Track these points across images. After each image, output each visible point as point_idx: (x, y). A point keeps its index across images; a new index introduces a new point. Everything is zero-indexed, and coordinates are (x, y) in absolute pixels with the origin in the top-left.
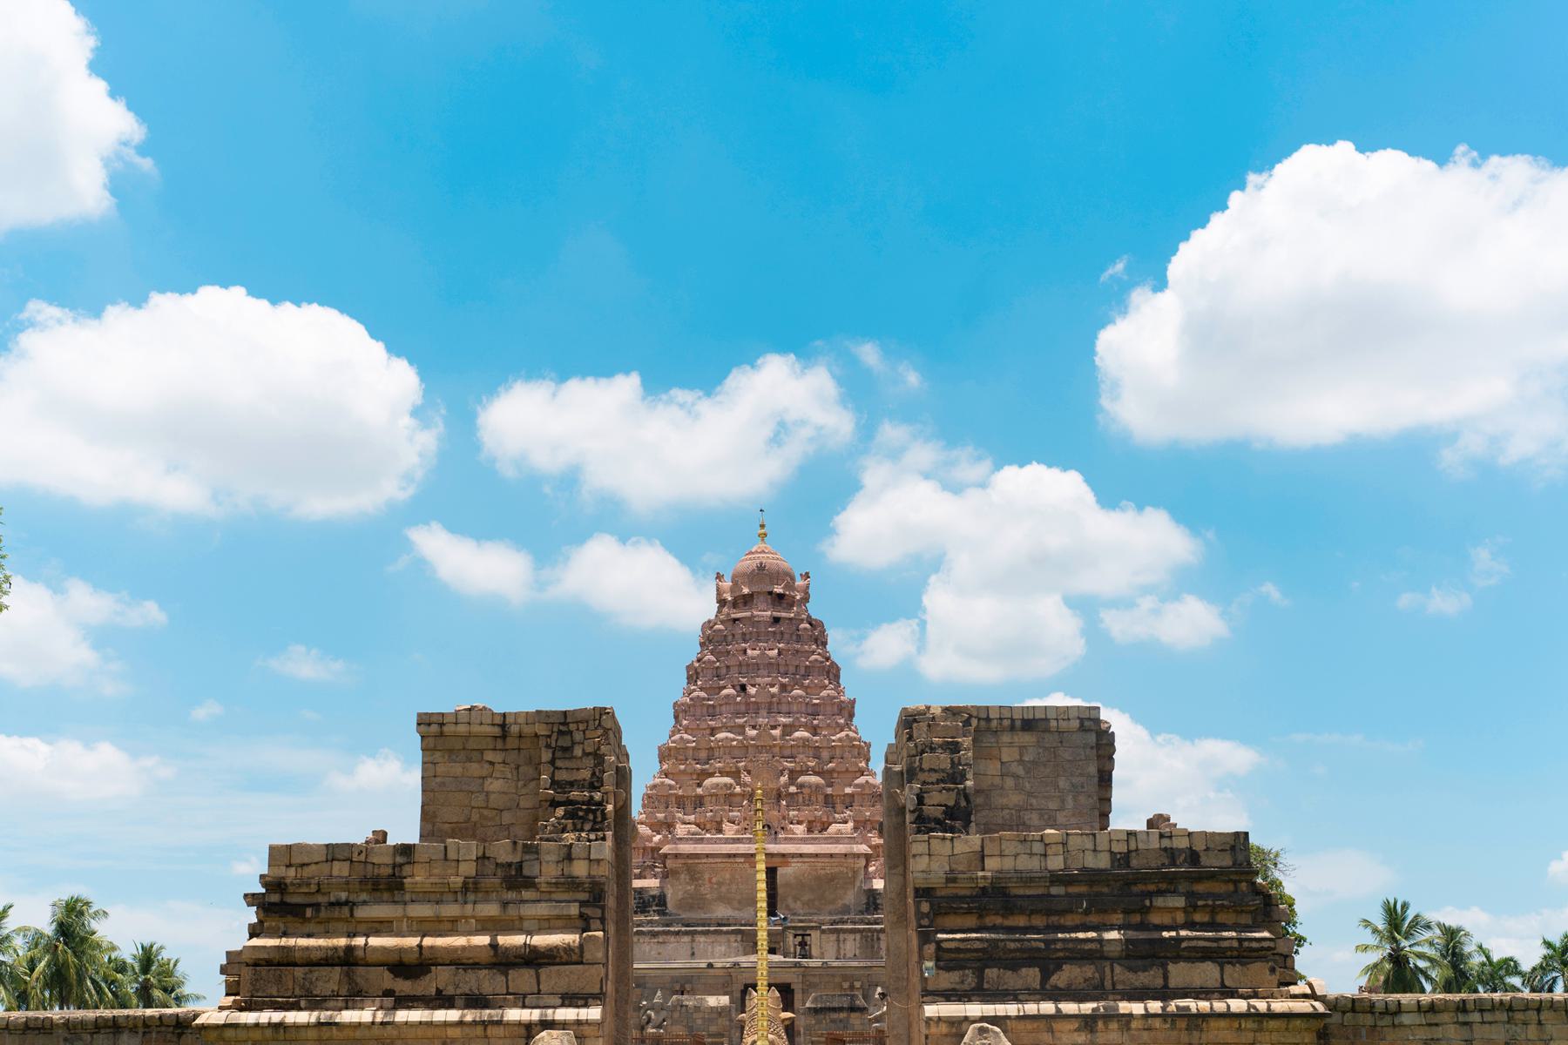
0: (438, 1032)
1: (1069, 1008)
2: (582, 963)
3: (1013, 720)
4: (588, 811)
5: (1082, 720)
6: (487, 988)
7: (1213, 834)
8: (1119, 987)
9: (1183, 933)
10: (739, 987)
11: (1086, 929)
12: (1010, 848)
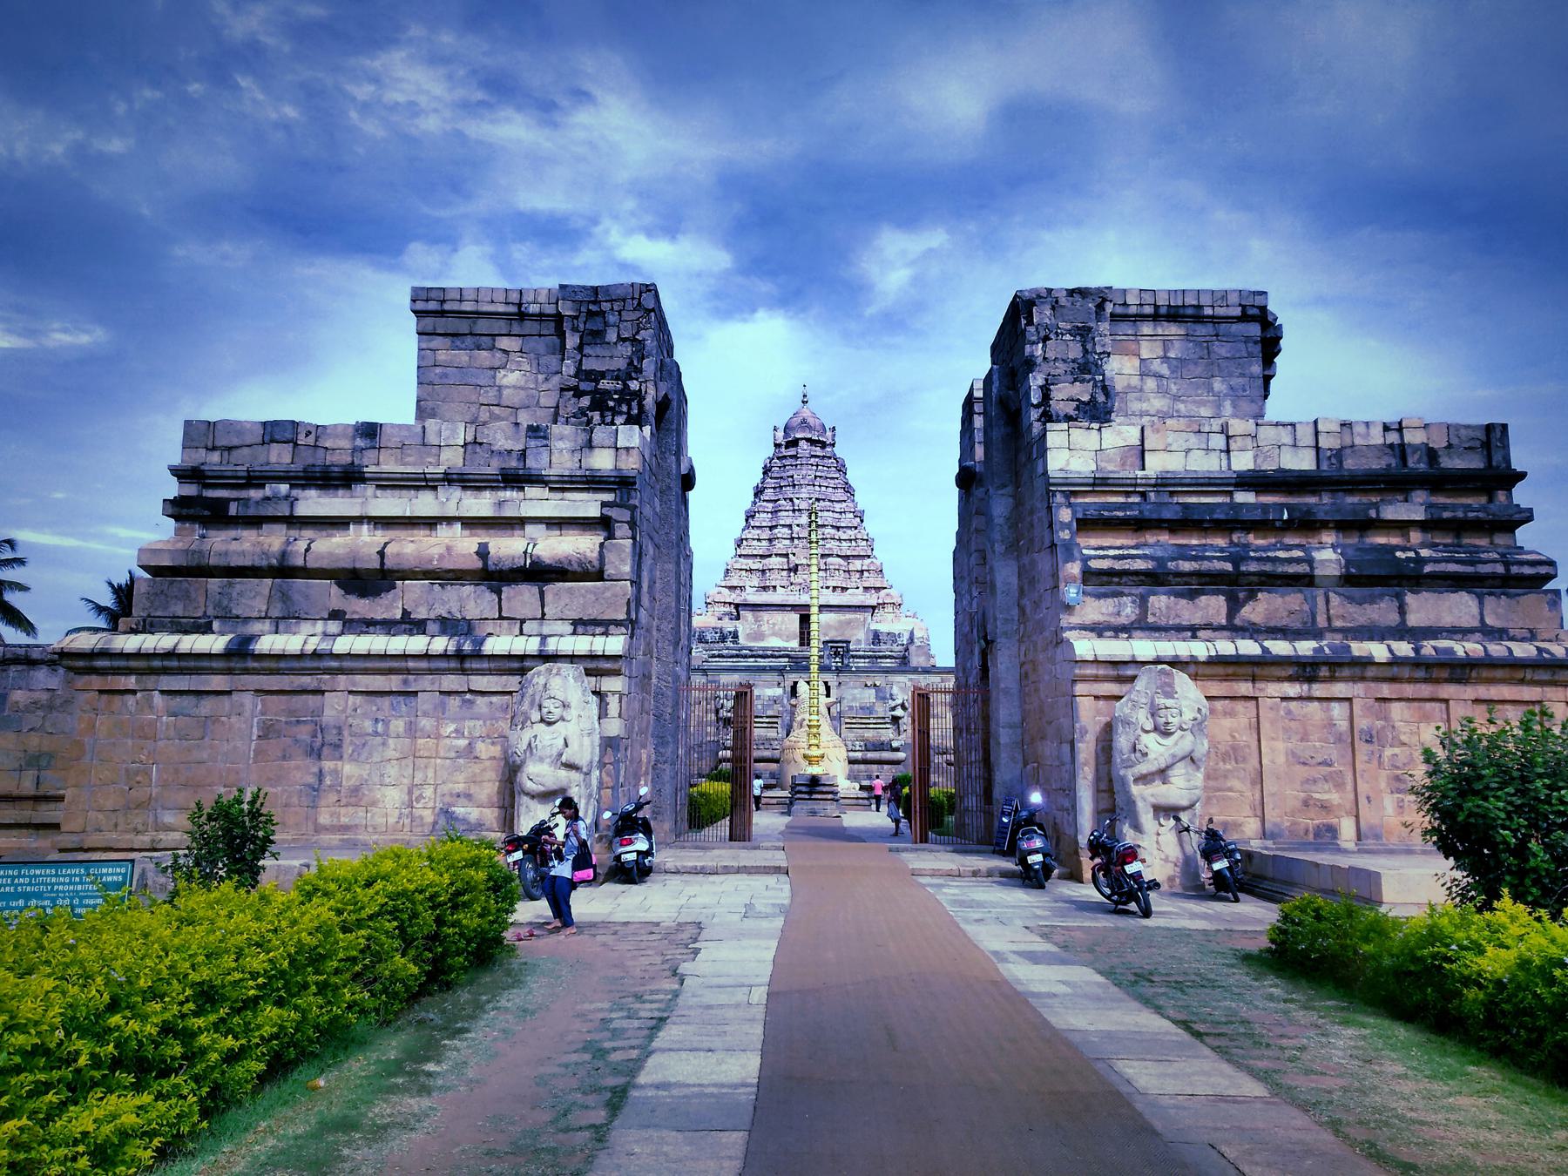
0: (395, 664)
1: (1280, 647)
2: (602, 579)
3: (1156, 307)
4: (619, 402)
5: (1244, 307)
6: (472, 612)
7: (1458, 427)
8: (1338, 624)
9: (1425, 553)
10: (789, 684)
11: (1289, 548)
12: (1178, 441)
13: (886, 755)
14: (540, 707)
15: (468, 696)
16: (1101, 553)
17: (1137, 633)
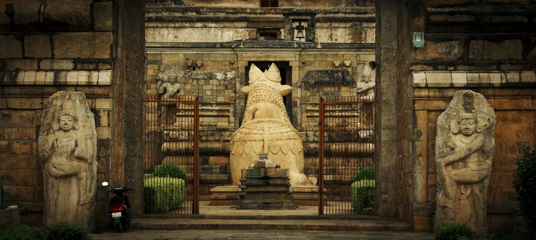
13: (352, 147)
14: (59, 120)
15: (6, 112)
16: (439, 10)
17: (461, 67)
